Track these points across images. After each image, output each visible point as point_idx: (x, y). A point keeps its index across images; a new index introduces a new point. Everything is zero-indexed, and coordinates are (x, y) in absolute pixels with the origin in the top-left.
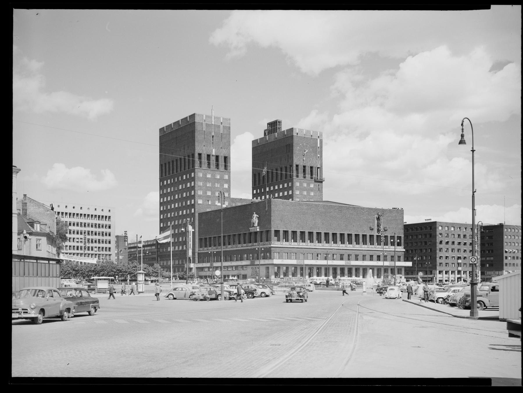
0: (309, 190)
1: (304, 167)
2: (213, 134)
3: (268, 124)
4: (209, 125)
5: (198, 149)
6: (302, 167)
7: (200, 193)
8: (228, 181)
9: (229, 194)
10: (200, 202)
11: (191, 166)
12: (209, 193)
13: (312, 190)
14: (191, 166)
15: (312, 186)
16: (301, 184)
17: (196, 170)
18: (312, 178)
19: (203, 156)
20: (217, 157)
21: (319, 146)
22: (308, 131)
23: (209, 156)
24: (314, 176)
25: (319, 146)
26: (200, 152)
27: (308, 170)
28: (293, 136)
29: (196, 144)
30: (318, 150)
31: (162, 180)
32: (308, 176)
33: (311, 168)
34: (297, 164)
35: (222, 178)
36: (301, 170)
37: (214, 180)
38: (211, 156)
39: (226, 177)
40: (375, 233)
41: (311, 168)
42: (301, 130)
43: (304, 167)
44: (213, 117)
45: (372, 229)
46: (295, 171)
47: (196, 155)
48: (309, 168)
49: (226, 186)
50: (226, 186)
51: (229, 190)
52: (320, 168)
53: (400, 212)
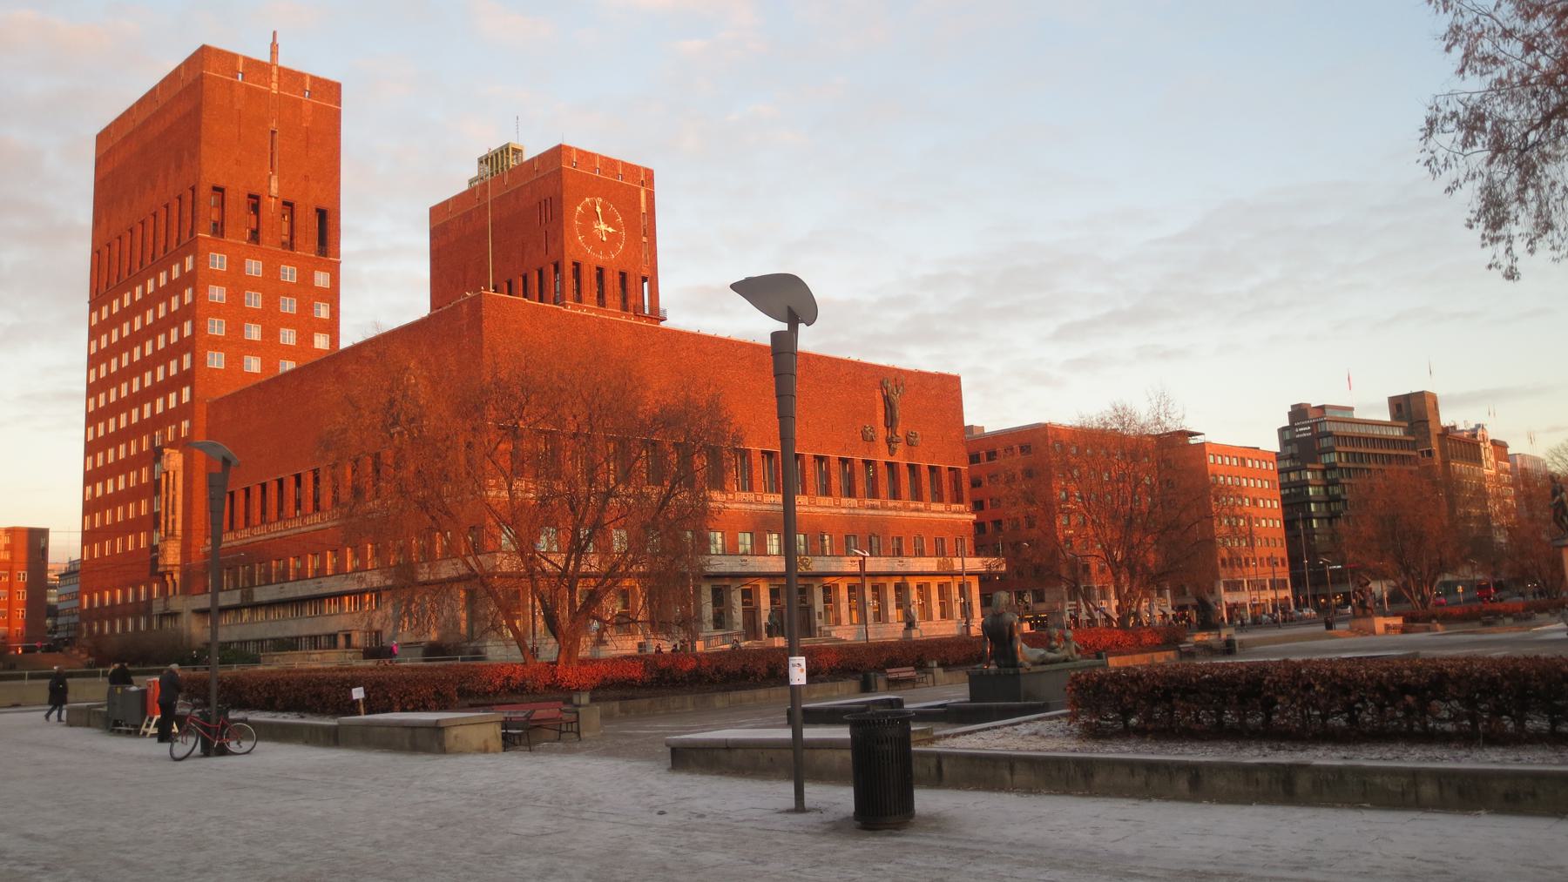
1: (600, 272)
2: (273, 125)
3: (481, 162)
4: (260, 93)
5: (214, 169)
6: (594, 271)
7: (217, 328)
8: (332, 296)
9: (335, 340)
10: (216, 360)
11: (186, 238)
12: (254, 333)
14: (186, 238)
17: (201, 246)
18: (625, 308)
19: (229, 196)
20: (289, 205)
21: (644, 210)
22: (610, 163)
23: (255, 202)
24: (631, 302)
25: (644, 210)
26: (221, 183)
27: (612, 281)
28: (561, 169)
29: (204, 148)
30: (644, 222)
31: (95, 305)
32: (614, 298)
33: (623, 276)
35: (306, 279)
36: (588, 278)
37: (272, 287)
38: (263, 204)
40: (882, 457)
41: (623, 276)
42: (585, 156)
43: (600, 272)
44: (275, 71)
45: (868, 439)
46: (570, 283)
47: (204, 191)
48: (617, 277)
50: (323, 312)
51: (332, 327)
52: (652, 278)
53: (946, 389)
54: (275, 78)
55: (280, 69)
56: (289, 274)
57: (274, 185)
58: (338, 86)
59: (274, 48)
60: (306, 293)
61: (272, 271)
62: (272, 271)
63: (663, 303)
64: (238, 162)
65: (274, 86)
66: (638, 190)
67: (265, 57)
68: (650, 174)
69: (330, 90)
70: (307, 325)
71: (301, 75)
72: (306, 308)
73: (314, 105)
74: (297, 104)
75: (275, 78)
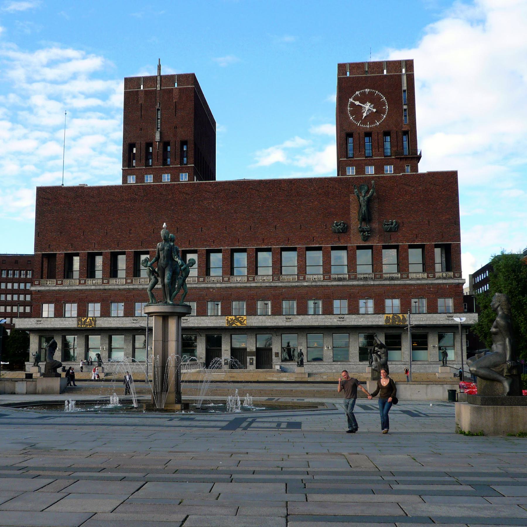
23: (150, 144)
34: (349, 131)
55: (161, 77)
64: (141, 129)
65: (158, 86)
67: (155, 73)
71: (173, 76)
73: (180, 89)
74: (171, 91)
75: (159, 82)
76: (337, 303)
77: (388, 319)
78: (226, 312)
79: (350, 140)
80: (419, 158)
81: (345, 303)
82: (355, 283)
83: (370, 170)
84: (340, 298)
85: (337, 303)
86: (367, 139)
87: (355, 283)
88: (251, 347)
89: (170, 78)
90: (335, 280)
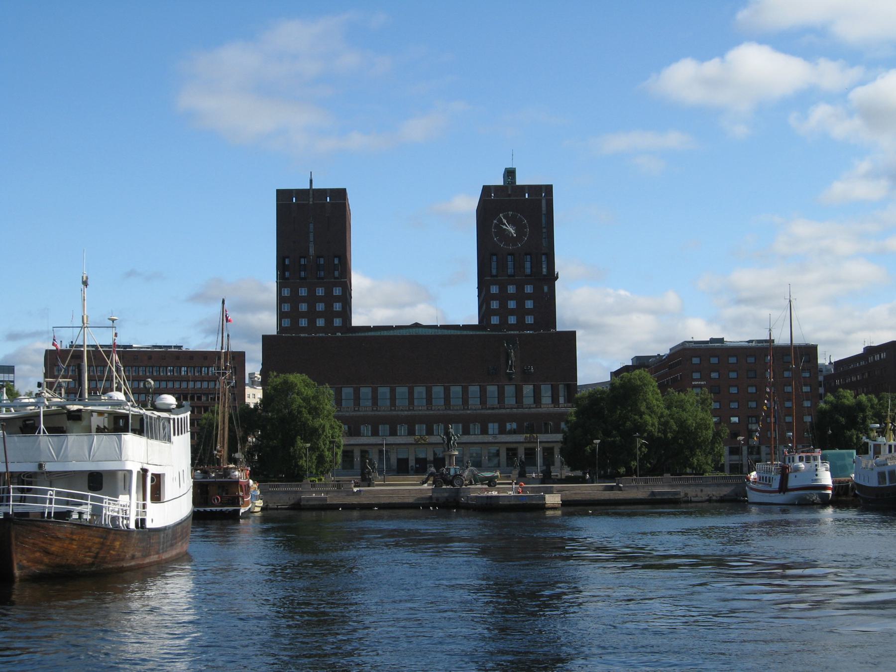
0: (521, 297)
13: (529, 297)
15: (529, 289)
16: (503, 289)
35: (329, 292)
39: (337, 291)
49: (337, 307)
54: (311, 196)
56: (320, 292)
57: (312, 251)
58: (344, 190)
59: (311, 181)
60: (329, 299)
61: (312, 292)
62: (312, 292)
63: (556, 270)
65: (311, 199)
66: (540, 201)
68: (549, 189)
69: (340, 195)
70: (329, 315)
72: (329, 306)
75: (311, 196)
76: (490, 425)
77: (526, 437)
78: (411, 432)
79: (494, 258)
80: (557, 278)
81: (496, 425)
82: (503, 411)
83: (511, 289)
84: (493, 422)
85: (490, 425)
86: (509, 258)
87: (503, 411)
88: (430, 457)
89: (323, 192)
90: (489, 409)
